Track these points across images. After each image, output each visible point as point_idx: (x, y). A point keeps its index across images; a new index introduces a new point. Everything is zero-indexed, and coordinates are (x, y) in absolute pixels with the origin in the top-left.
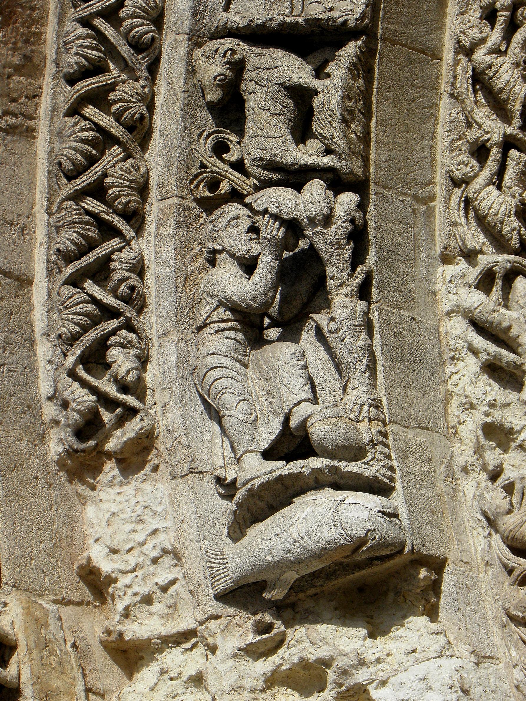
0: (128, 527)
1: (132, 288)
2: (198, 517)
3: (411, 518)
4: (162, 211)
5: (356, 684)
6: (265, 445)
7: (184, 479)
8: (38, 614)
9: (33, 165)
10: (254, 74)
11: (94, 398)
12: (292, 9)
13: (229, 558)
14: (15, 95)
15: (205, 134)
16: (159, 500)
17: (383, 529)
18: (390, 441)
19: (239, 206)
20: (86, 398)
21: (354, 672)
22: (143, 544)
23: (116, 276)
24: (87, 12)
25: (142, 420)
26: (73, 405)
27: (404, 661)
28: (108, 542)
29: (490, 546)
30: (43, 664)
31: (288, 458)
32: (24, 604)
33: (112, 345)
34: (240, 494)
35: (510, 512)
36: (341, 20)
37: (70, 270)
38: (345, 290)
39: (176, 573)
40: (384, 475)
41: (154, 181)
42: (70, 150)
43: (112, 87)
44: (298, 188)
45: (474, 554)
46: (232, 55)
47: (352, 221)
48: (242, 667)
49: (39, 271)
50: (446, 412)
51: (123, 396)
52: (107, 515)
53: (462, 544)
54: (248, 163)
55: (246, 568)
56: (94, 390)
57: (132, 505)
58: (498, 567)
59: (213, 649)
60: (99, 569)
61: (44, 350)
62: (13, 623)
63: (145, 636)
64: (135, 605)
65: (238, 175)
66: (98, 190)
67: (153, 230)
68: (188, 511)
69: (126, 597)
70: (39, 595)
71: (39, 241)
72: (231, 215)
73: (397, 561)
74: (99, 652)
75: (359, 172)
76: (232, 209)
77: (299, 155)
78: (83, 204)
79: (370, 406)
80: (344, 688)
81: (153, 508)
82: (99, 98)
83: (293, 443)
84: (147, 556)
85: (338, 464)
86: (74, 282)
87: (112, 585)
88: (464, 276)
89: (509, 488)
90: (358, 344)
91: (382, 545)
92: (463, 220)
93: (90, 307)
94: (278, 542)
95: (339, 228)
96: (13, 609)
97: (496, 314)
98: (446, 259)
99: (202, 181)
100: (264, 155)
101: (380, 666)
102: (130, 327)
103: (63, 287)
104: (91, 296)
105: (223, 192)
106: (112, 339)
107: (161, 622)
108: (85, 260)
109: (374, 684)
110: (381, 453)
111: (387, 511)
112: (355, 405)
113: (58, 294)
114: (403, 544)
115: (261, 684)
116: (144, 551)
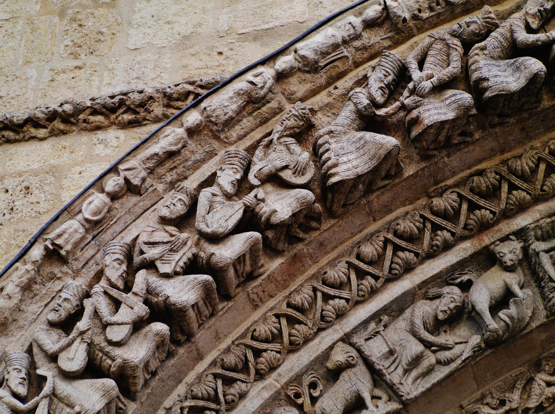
4: (271, 384)
9: (245, 319)
10: (352, 376)
12: (389, 367)
14: (265, 290)
15: (313, 375)
23: (232, 391)
24: (320, 288)
36: (402, 394)
37: (220, 371)
41: (279, 370)
42: (263, 330)
43: (300, 322)
46: (352, 360)
49: (208, 359)
54: (318, 404)
61: (181, 389)
66: (257, 353)
67: (261, 387)
71: (219, 348)
78: (247, 352)
82: (292, 321)
86: (216, 376)
93: (212, 392)
99: (295, 390)
103: (211, 375)
104: (216, 387)
105: (298, 402)
108: (227, 373)
113: (207, 375)
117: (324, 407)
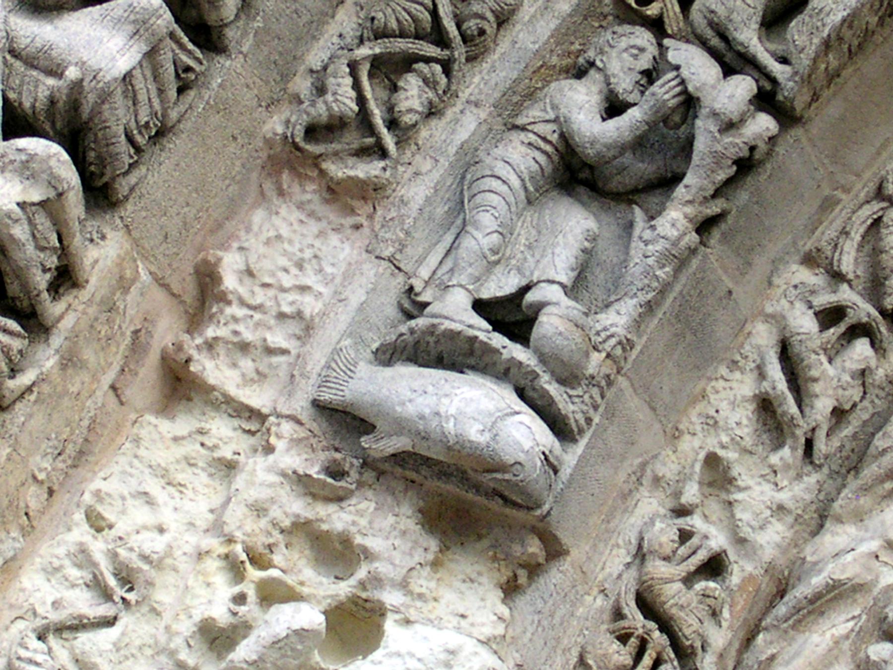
0: (283, 262)
1: (482, 32)
2: (361, 308)
5: (379, 601)
6: (485, 295)
7: (377, 261)
8: (128, 274)
11: (356, 109)
13: (358, 375)
16: (336, 261)
19: (654, 41)
20: (348, 102)
21: (388, 588)
22: (283, 290)
25: (384, 169)
26: (329, 97)
27: (445, 618)
29: (620, 576)
30: (92, 326)
31: (498, 326)
32: (122, 252)
33: (415, 70)
34: (420, 322)
35: (667, 559)
38: (689, 210)
40: (576, 421)
44: (728, 71)
45: (597, 570)
47: (752, 149)
48: (282, 492)
50: (685, 412)
51: (384, 131)
52: (272, 233)
55: (367, 398)
56: (361, 100)
58: (609, 604)
59: (269, 449)
62: (96, 261)
63: (212, 381)
64: (227, 343)
65: (677, 9)
68: (356, 296)
69: (224, 328)
70: (143, 256)
72: (639, 42)
73: (520, 515)
74: (153, 358)
75: (799, 105)
76: (643, 37)
77: (755, 41)
79: (620, 343)
80: (364, 595)
83: (512, 316)
84: (279, 305)
85: (541, 373)
87: (221, 304)
88: (813, 292)
89: (685, 536)
90: (657, 273)
91: (520, 488)
92: (858, 238)
93: (425, 17)
94: (420, 400)
95: (735, 144)
96: (107, 249)
97: (813, 356)
98: (810, 260)
100: (721, 11)
101: (419, 604)
102: (447, 67)
105: (649, 13)
106: (421, 66)
107: (239, 380)
109: (397, 617)
110: (591, 397)
111: (551, 459)
112: (605, 329)
114: (539, 506)
115: (287, 523)
116: (279, 298)
117: (713, 7)
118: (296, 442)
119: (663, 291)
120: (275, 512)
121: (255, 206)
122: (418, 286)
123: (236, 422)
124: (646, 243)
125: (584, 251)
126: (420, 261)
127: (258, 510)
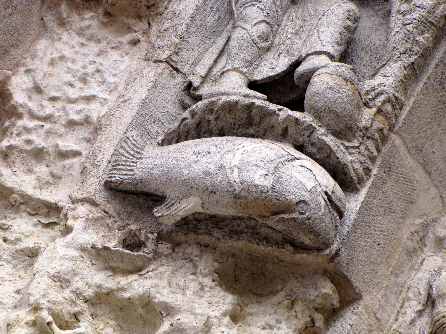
0: (68, 78)
2: (144, 104)
3: (355, 226)
7: (155, 65)
13: (146, 155)
16: (117, 72)
17: (319, 210)
18: (385, 149)
28: (39, 76)
39: (83, 148)
40: (355, 170)
45: (391, 321)
48: (83, 265)
52: (56, 55)
53: (387, 301)
55: (156, 171)
57: (87, 60)
59: (68, 230)
60: (11, 94)
63: (9, 184)
64: (21, 151)
68: (138, 94)
69: (17, 139)
79: (388, 100)
81: (106, 76)
84: (67, 114)
85: (317, 127)
87: (13, 119)
90: (417, 39)
94: (205, 160)
107: (35, 183)
110: (367, 149)
111: (333, 198)
112: (373, 89)
114: (327, 245)
115: (89, 293)
116: (67, 109)
118: (91, 222)
119: (426, 55)
120: (78, 283)
121: (38, 37)
122: (196, 82)
123: (35, 220)
124: (404, 14)
125: (347, 28)
126: (195, 64)
127: (61, 280)
